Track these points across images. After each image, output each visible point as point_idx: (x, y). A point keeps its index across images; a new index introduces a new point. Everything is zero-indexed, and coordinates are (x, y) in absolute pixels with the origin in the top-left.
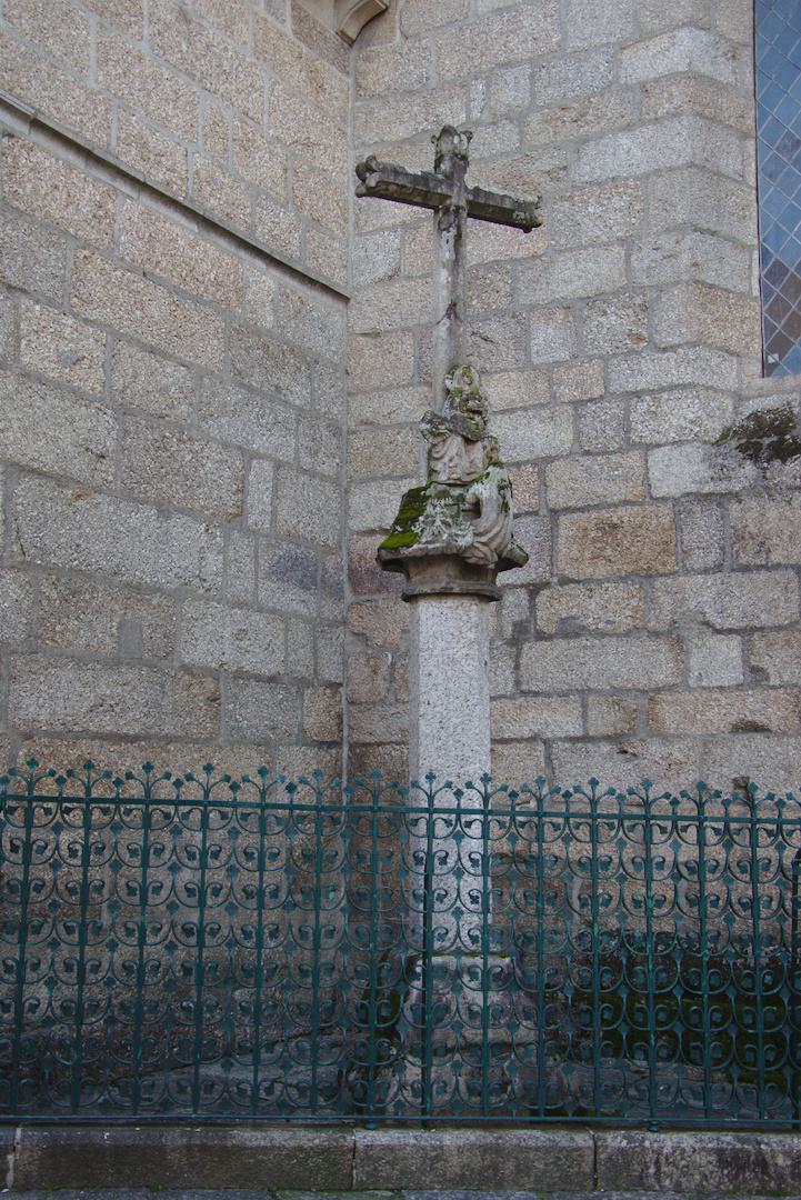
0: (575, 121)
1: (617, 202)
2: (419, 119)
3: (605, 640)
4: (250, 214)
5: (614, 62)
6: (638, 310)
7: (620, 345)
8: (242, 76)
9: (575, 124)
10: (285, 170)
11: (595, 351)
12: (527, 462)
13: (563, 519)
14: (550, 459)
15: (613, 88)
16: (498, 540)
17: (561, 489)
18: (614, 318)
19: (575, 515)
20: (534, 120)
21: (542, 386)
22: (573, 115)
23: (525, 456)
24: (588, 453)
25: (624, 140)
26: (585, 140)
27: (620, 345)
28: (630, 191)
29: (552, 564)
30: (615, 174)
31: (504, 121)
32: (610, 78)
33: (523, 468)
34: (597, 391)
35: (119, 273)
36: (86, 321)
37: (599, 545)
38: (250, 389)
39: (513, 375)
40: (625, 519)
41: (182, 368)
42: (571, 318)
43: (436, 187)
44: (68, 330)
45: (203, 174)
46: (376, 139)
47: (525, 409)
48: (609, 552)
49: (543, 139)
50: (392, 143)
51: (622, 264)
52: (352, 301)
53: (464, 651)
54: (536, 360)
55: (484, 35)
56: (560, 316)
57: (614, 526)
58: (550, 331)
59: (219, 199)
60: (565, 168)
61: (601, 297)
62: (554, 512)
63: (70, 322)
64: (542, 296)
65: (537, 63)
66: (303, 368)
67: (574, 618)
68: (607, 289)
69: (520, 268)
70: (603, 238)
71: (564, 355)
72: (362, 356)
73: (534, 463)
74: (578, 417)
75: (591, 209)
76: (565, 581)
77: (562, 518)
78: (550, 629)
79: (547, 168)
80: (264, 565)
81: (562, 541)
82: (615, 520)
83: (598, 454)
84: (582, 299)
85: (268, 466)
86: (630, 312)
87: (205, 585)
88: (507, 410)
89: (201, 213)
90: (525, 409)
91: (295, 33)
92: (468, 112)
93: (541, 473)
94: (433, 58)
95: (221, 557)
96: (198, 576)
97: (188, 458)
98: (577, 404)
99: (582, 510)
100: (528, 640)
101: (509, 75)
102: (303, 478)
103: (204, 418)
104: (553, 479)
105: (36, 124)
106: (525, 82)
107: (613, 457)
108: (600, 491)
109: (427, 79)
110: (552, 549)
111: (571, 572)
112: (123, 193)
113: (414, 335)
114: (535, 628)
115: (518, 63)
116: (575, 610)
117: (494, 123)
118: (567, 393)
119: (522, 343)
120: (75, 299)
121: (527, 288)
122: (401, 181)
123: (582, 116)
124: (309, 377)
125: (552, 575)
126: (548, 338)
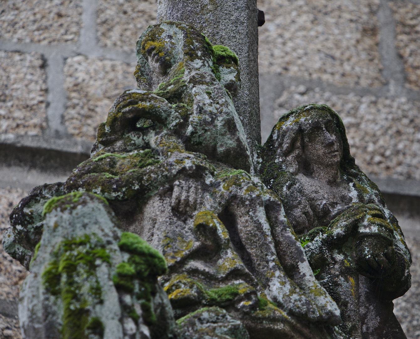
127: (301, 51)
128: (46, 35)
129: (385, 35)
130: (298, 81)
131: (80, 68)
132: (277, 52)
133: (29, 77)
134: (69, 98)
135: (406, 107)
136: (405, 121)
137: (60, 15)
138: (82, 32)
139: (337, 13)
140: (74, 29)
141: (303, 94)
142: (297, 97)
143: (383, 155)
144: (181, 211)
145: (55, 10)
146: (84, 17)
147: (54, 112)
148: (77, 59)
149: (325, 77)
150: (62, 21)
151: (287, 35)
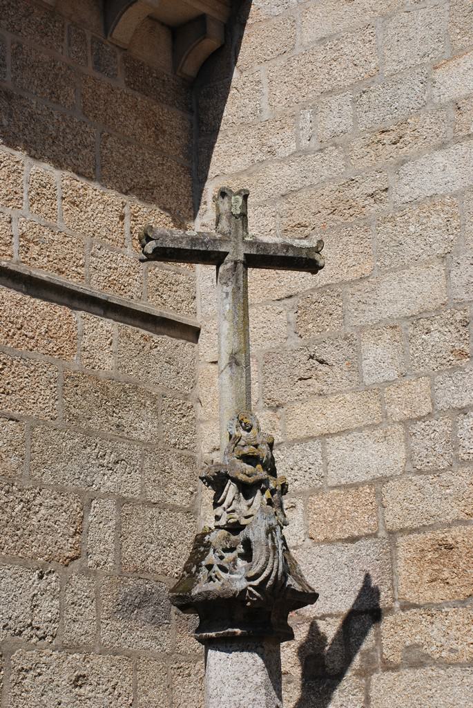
0: (394, 144)
1: (436, 220)
2: (255, 150)
3: (450, 670)
4: (82, 266)
5: (428, 81)
6: (459, 326)
7: (445, 361)
8: (70, 137)
9: (394, 146)
10: (122, 218)
11: (422, 369)
12: (364, 483)
13: (401, 540)
14: (383, 480)
15: (428, 108)
16: (270, 583)
17: (397, 509)
18: (438, 334)
19: (411, 536)
20: (357, 145)
21: (374, 406)
22: (392, 136)
23: (363, 478)
24: (420, 472)
25: (440, 158)
26: (403, 162)
27: (445, 361)
28: (446, 208)
29: (394, 589)
30: (433, 192)
31: (331, 148)
32: (425, 97)
33: (361, 489)
34: (426, 409)
37: (436, 567)
38: (88, 432)
39: (348, 397)
40: (459, 539)
41: (11, 422)
42: (397, 338)
46: (218, 172)
47: (360, 430)
48: (446, 574)
49: (365, 162)
50: (232, 175)
51: (442, 281)
52: (202, 331)
53: (252, 696)
54: (368, 380)
55: (310, 65)
56: (387, 335)
57: (450, 548)
58: (379, 351)
59: (48, 256)
60: (386, 190)
61: (424, 315)
62: (391, 533)
64: (369, 317)
65: (361, 89)
66: (148, 403)
67: (418, 646)
68: (431, 306)
69: (350, 290)
70: (424, 256)
71: (392, 374)
72: (212, 385)
73: (371, 483)
74: (408, 436)
75: (412, 229)
76: (406, 606)
77: (400, 540)
78: (396, 658)
79: (371, 191)
80: (108, 604)
81: (401, 563)
82: (450, 541)
83: (428, 473)
84: (408, 318)
85: (110, 505)
86: (452, 328)
87: (38, 633)
88: (344, 431)
89: (27, 273)
90: (360, 430)
91: (128, 84)
92: (298, 141)
93: (378, 494)
94: (266, 90)
96: (31, 624)
97: (18, 508)
98: (407, 422)
99: (417, 530)
100: (375, 670)
101: (334, 101)
102: (152, 512)
103: (37, 467)
104: (389, 499)
106: (348, 109)
107: (444, 476)
108: (433, 511)
109: (261, 111)
110: (392, 572)
111: (411, 597)
113: (257, 361)
114: (382, 657)
115: (343, 90)
116: (418, 637)
117: (321, 150)
118: (398, 412)
119: (354, 366)
121: (356, 310)
123: (401, 138)
124: (155, 411)
125: (394, 600)
126: (378, 357)
128: (11, 204)
133: (6, 228)
134: (20, 241)
137: (16, 193)
138: (24, 203)
147: (15, 248)
148: (23, 219)
150: (17, 196)
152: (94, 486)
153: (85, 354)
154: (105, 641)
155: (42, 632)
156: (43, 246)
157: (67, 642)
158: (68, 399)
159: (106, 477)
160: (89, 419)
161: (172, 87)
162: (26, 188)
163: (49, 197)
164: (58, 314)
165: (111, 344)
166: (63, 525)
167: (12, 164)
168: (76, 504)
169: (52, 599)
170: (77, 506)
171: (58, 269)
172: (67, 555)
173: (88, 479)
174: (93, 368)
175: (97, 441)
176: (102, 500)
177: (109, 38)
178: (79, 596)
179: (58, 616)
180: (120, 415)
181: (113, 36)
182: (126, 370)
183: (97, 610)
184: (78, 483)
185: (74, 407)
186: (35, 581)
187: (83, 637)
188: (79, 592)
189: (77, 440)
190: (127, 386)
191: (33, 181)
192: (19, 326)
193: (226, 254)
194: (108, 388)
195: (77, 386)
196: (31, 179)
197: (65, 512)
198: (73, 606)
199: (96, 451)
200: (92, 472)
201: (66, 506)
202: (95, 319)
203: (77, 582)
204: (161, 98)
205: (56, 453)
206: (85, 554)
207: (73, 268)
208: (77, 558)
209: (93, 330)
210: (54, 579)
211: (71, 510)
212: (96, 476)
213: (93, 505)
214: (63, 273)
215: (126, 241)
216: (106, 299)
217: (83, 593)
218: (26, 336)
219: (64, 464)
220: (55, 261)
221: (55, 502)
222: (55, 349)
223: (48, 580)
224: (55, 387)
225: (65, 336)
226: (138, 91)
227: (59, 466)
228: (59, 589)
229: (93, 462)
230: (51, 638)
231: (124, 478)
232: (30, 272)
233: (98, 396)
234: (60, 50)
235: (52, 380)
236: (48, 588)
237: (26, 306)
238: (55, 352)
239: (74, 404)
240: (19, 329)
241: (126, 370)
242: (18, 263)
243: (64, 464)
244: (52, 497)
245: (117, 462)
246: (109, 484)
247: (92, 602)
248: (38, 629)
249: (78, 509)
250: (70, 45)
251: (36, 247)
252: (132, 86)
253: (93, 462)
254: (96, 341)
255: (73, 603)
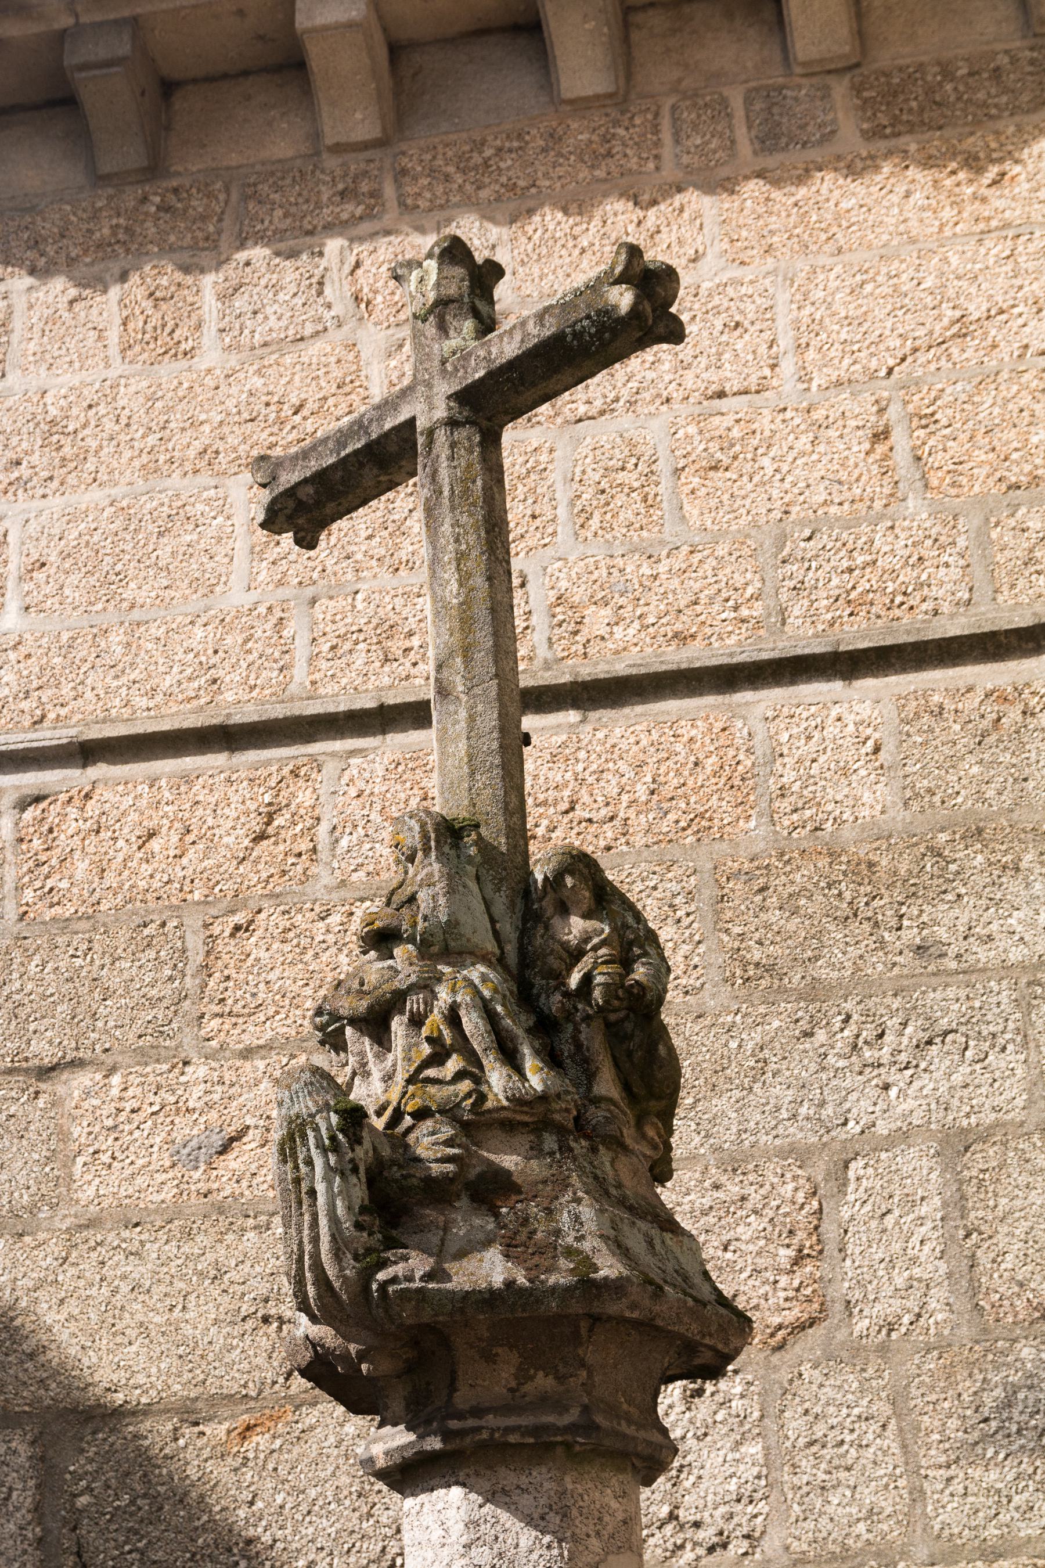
35: (335, 919)
36: (247, 1053)
38: (814, 992)
43: (380, 419)
44: (198, 1091)
45: (579, 595)
63: (202, 1071)
80: (942, 1423)
85: (917, 1163)
87: (701, 1535)
95: (754, 1449)
96: (672, 1517)
105: (87, 752)
112: (333, 754)
120: (215, 1023)
122: (314, 465)
127: (802, 484)
129: (899, 438)
130: (802, 523)
131: (562, 575)
132: (775, 494)
135: (927, 524)
136: (929, 542)
138: (559, 529)
139: (840, 423)
140: (550, 530)
141: (809, 539)
142: (802, 544)
143: (905, 594)
144: (416, 1022)
145: (529, 512)
146: (559, 511)
149: (833, 510)
150: (538, 522)
151: (785, 468)
152: (851, 1124)
153: (785, 805)
154: (945, 1525)
155: (712, 1530)
156: (622, 601)
157: (805, 1547)
158: (737, 930)
159: (893, 1092)
160: (817, 958)
161: (1030, 69)
162: (563, 496)
163: (636, 485)
164: (685, 739)
165: (877, 750)
166: (751, 1247)
167: (521, 460)
168: (790, 1186)
169: (738, 1444)
170: (796, 1189)
171: (676, 635)
172: (776, 1320)
173: (829, 1111)
174: (816, 829)
175: (848, 1006)
176: (884, 1155)
177: (798, 70)
178: (834, 1421)
179: (763, 1482)
180: (925, 918)
181: (801, 56)
182: (937, 799)
183: (904, 1447)
184: (791, 1130)
185: (760, 943)
186: (670, 1407)
187: (861, 1527)
188: (832, 1409)
189: (776, 1024)
190: (943, 837)
191: (584, 472)
192: (566, 806)
193: (411, 422)
194: (871, 865)
195: (762, 890)
196: (578, 470)
197: (755, 1212)
198: (814, 1449)
199: (846, 1033)
200: (837, 1089)
201: (755, 1198)
202: (813, 709)
203: (821, 1386)
204: (994, 111)
205: (708, 1074)
206: (839, 1307)
207: (723, 616)
208: (812, 1322)
209: (809, 738)
210: (738, 1390)
211: (774, 1204)
212: (854, 1096)
213: (851, 1174)
214: (693, 636)
215: (901, 485)
216: (829, 649)
217: (845, 1411)
218: (590, 821)
219: (737, 1094)
220: (664, 621)
221: (716, 1194)
222: (683, 824)
223: (719, 1398)
224: (688, 915)
225: (713, 780)
226: (911, 132)
227: (720, 1104)
228: (756, 1414)
229: (841, 1063)
230: (746, 1543)
231: (957, 1079)
232: (577, 674)
233: (840, 894)
234: (651, 165)
235: (677, 901)
236: (719, 1417)
237: (582, 755)
238: (684, 829)
239: (757, 935)
240: (567, 812)
241: (937, 799)
242: (547, 666)
243: (737, 1094)
244: (707, 1184)
245: (930, 1042)
246: (910, 1104)
247: (884, 1426)
248: (697, 1525)
249: (800, 1197)
250: (677, 142)
251: (603, 612)
252: (888, 131)
253: (841, 1063)
254: (822, 759)
255: (811, 1444)
